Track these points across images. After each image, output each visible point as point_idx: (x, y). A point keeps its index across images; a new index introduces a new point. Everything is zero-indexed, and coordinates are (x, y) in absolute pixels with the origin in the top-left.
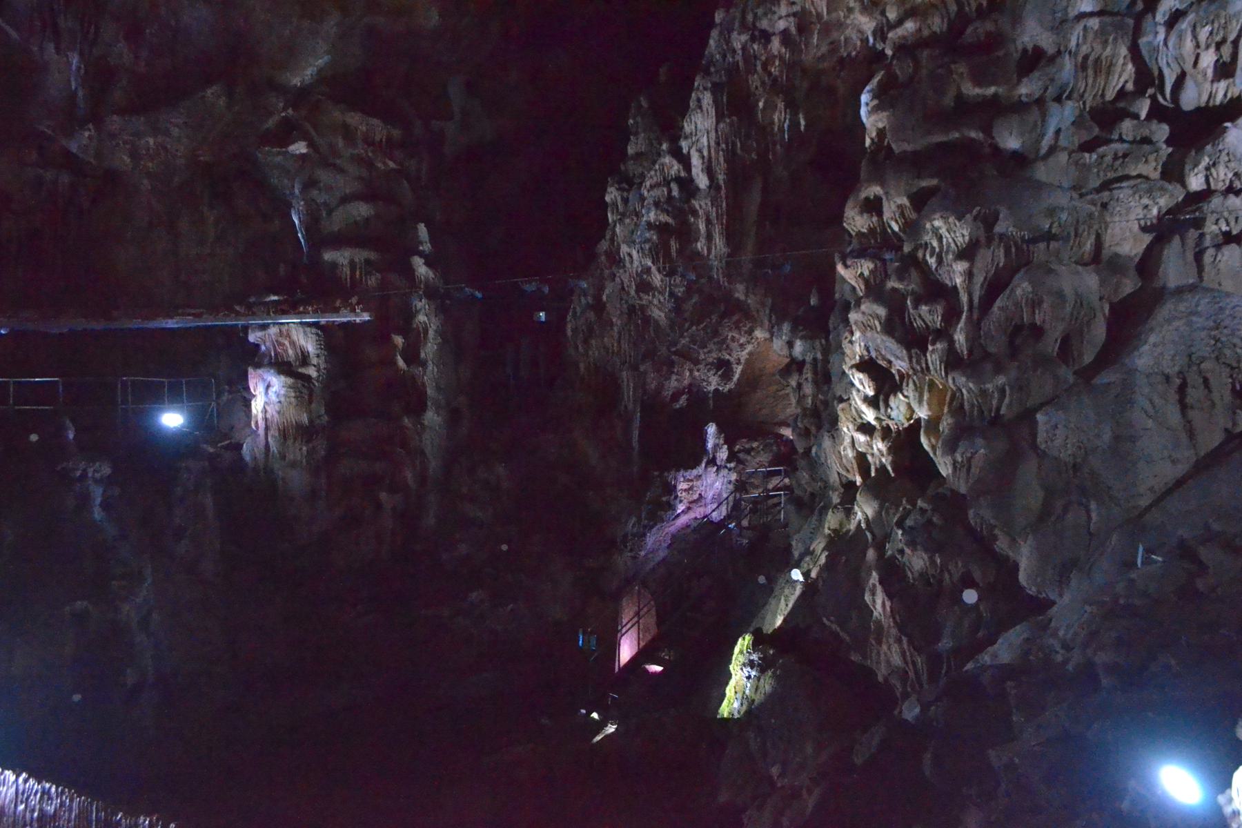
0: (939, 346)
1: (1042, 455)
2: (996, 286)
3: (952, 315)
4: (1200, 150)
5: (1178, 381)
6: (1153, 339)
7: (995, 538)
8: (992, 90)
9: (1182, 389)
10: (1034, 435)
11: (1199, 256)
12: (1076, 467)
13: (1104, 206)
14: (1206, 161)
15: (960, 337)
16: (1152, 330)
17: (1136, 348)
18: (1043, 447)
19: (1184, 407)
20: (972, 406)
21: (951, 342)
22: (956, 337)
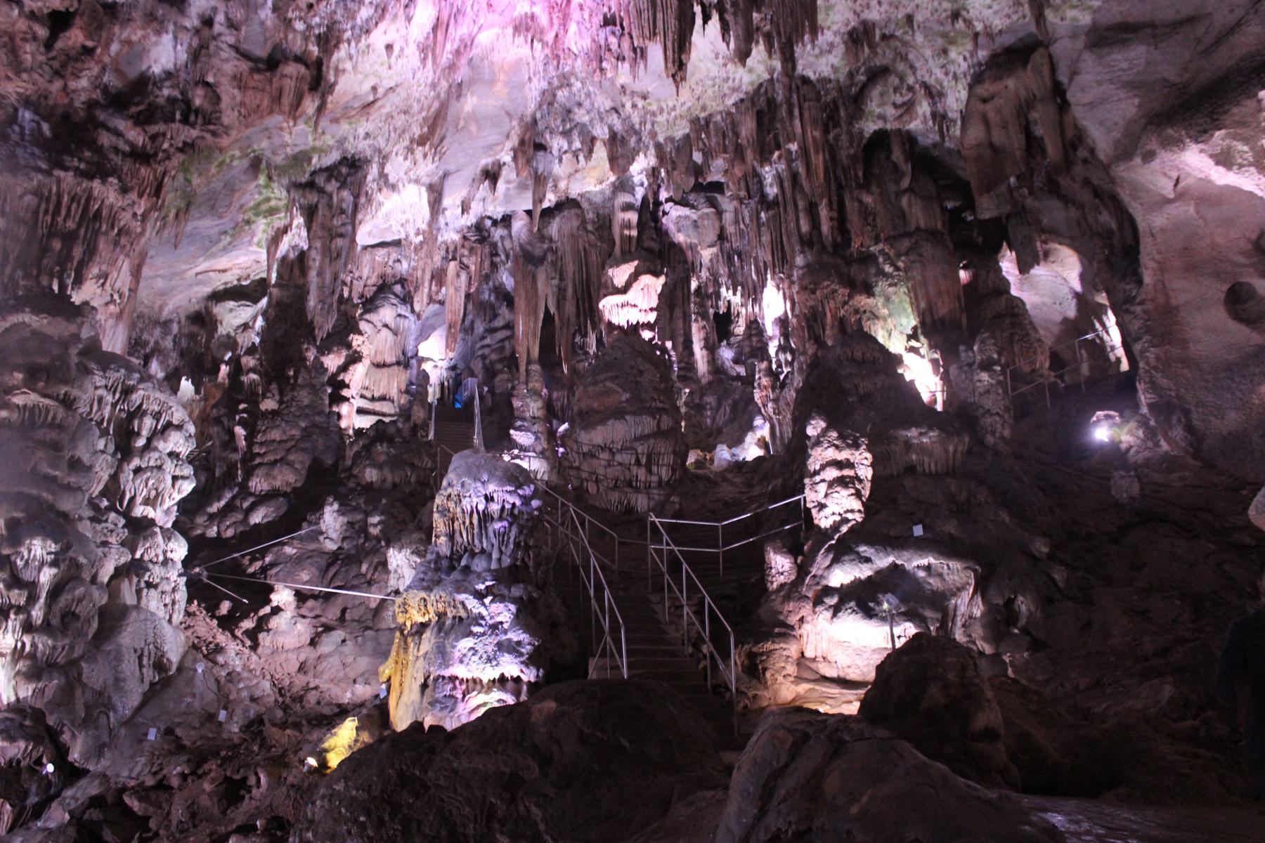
0: (21, 617)
1: (84, 685)
2: (56, 590)
3: (32, 599)
4: (145, 539)
5: (139, 652)
6: (129, 629)
7: (62, 732)
8: (57, 473)
9: (140, 658)
10: (80, 675)
11: (139, 592)
12: (101, 693)
13: (105, 556)
14: (148, 545)
15: (37, 613)
16: (128, 624)
17: (120, 633)
18: (85, 681)
19: (141, 666)
20: (44, 654)
21: (29, 615)
22: (34, 613)
